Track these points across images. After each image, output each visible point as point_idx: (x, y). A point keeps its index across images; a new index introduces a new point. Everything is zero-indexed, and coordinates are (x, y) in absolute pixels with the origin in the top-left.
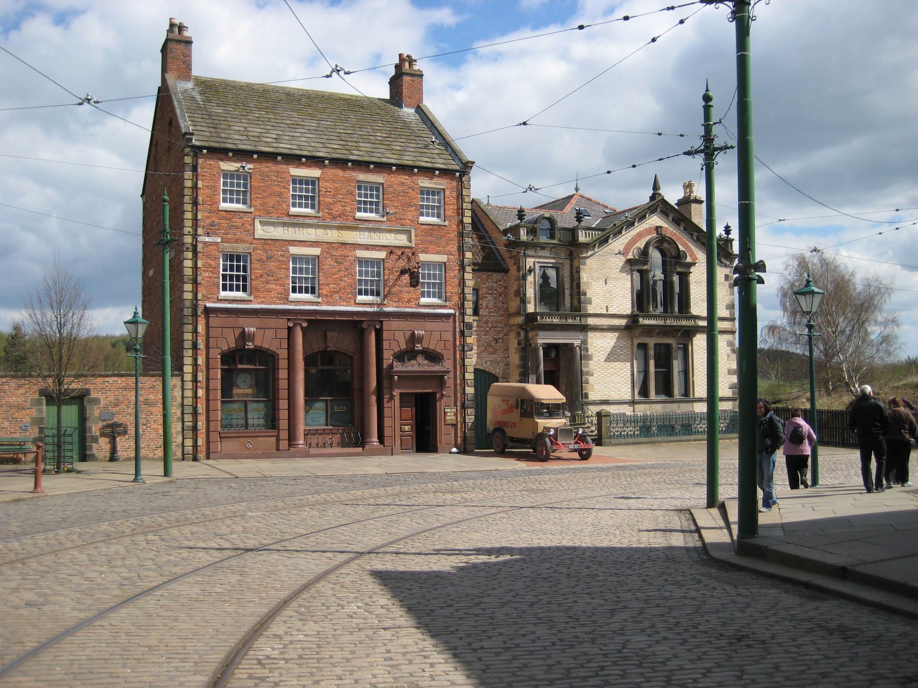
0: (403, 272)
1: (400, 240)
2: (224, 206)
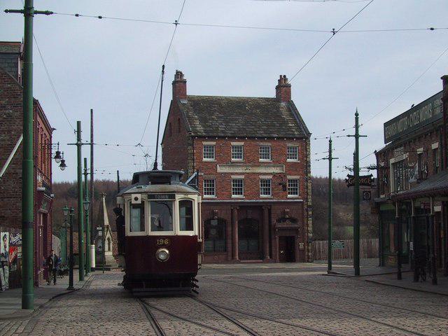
0: (280, 184)
1: (277, 170)
2: (205, 159)
